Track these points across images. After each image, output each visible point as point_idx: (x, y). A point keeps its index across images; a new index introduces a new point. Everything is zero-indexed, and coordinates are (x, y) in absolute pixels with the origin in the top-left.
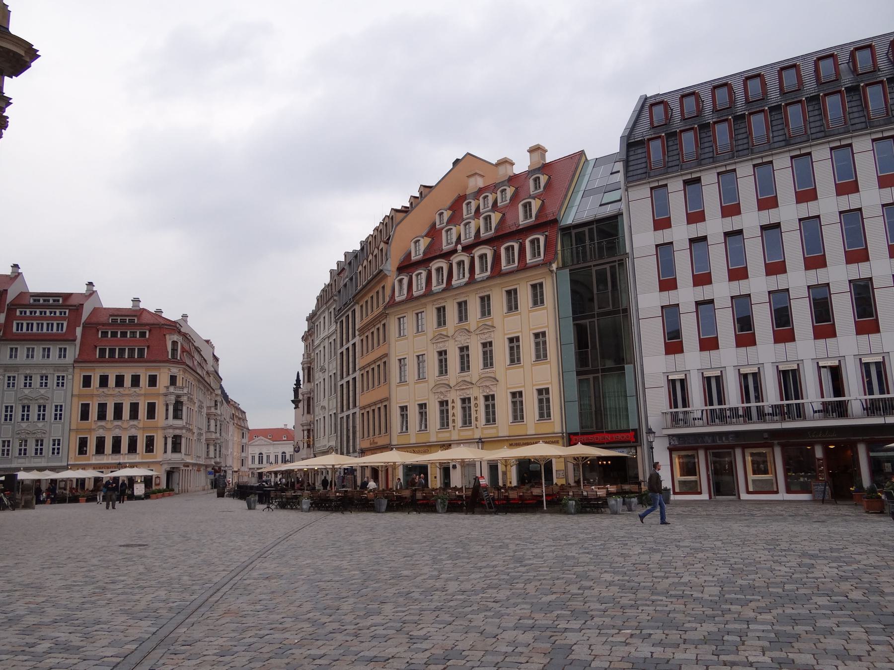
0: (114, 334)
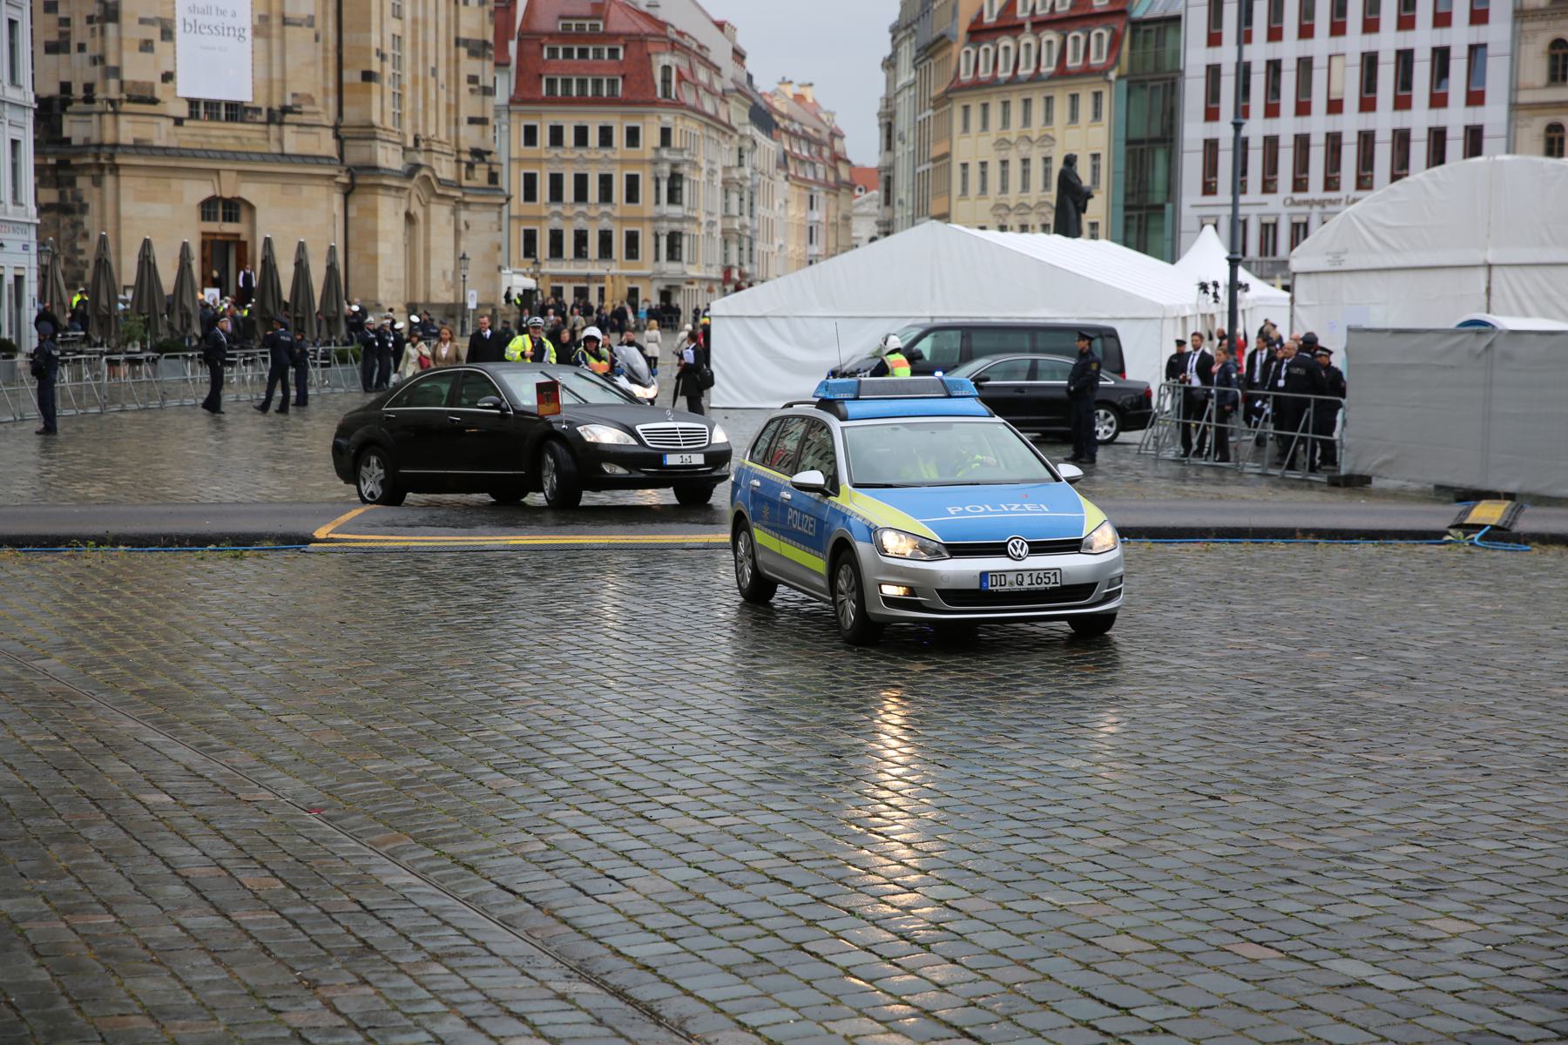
0: (568, 53)
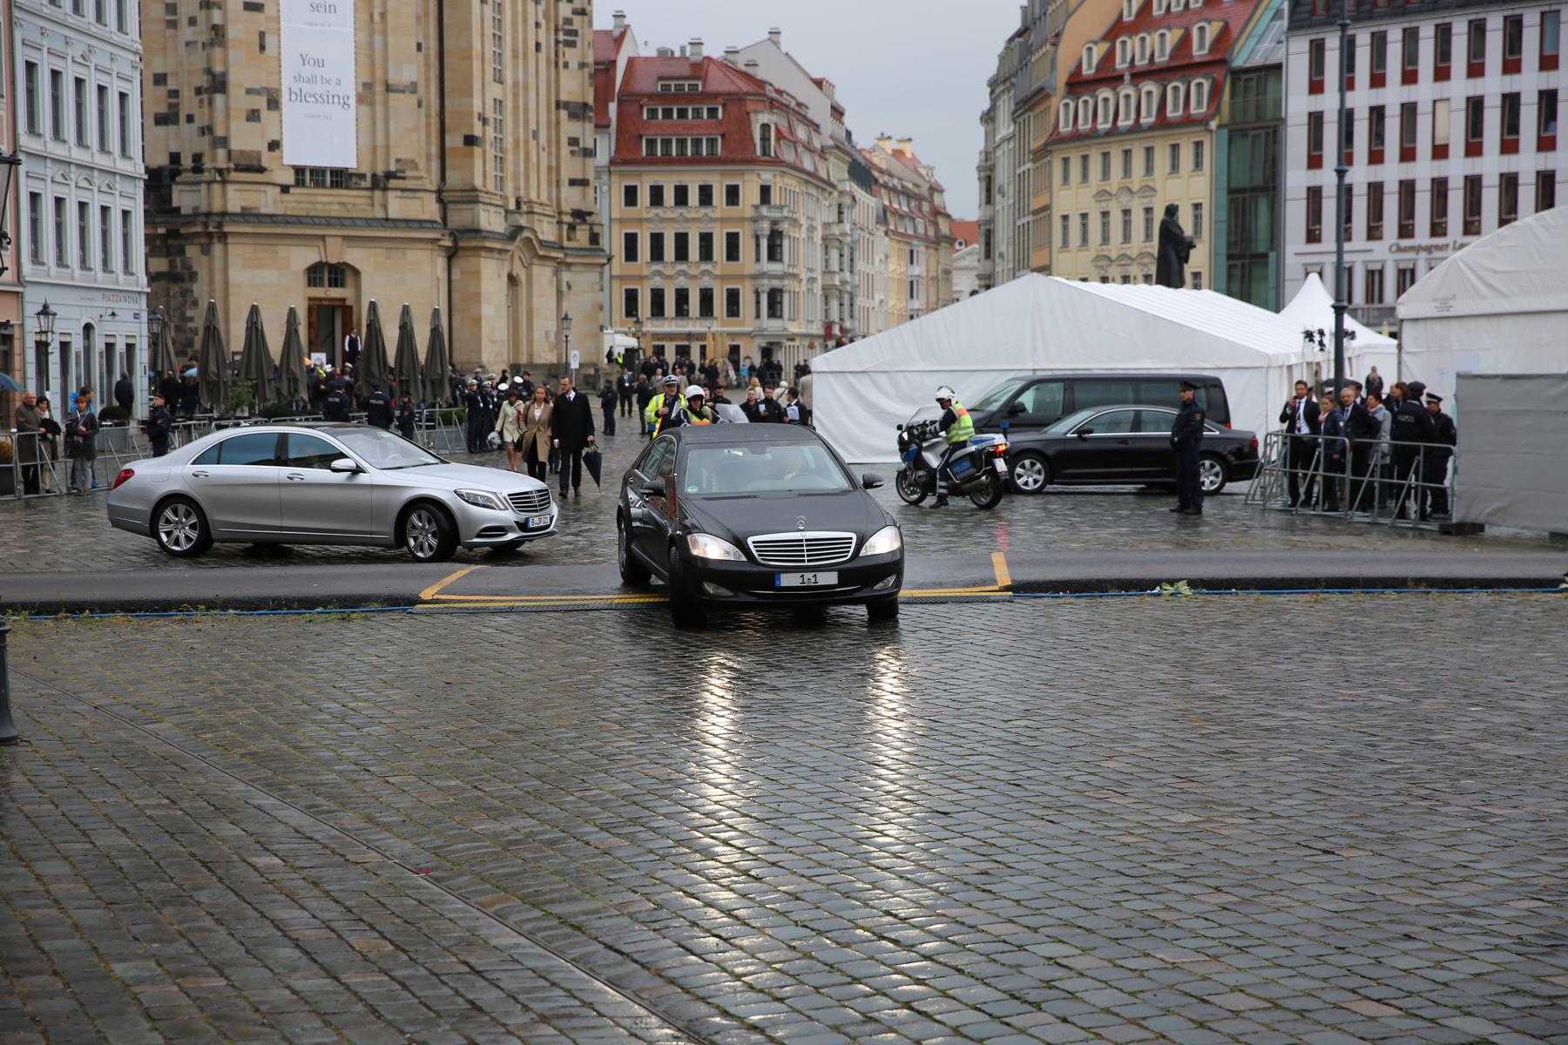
0: (668, 113)
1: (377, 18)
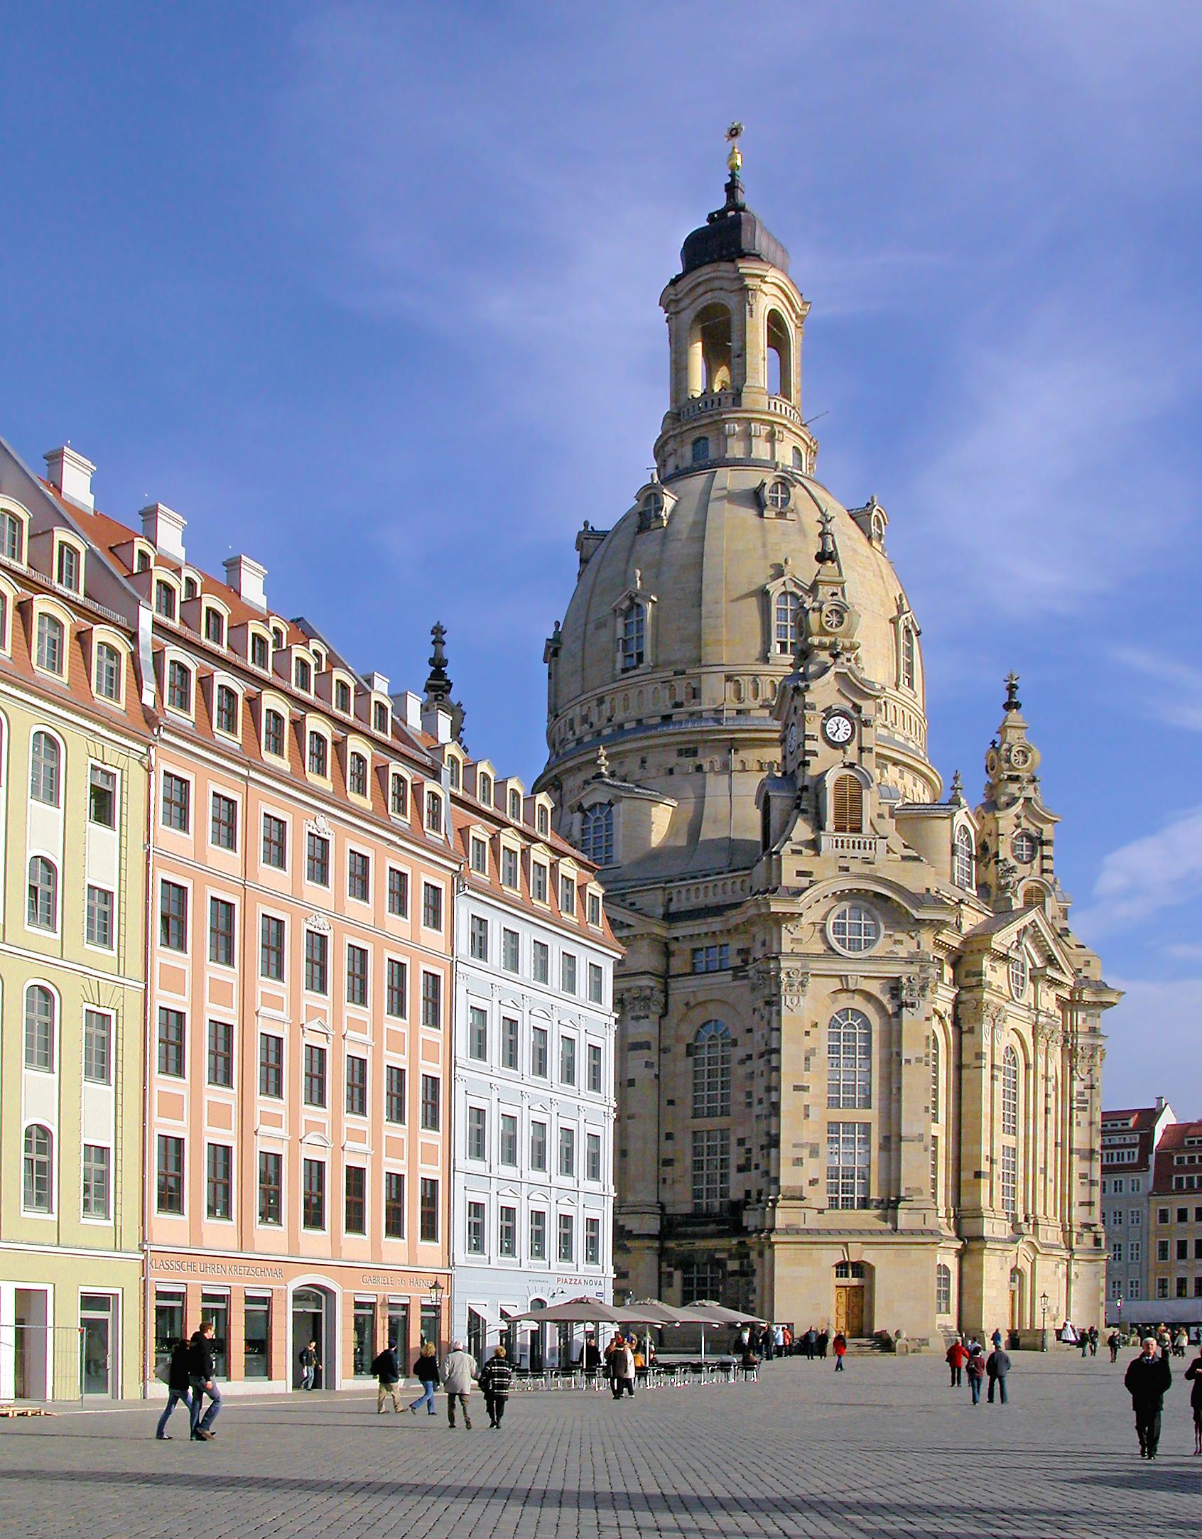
1: (894, 1091)
